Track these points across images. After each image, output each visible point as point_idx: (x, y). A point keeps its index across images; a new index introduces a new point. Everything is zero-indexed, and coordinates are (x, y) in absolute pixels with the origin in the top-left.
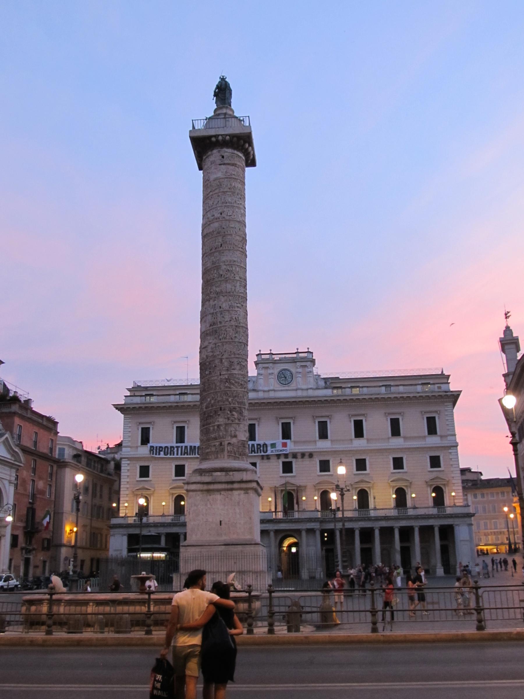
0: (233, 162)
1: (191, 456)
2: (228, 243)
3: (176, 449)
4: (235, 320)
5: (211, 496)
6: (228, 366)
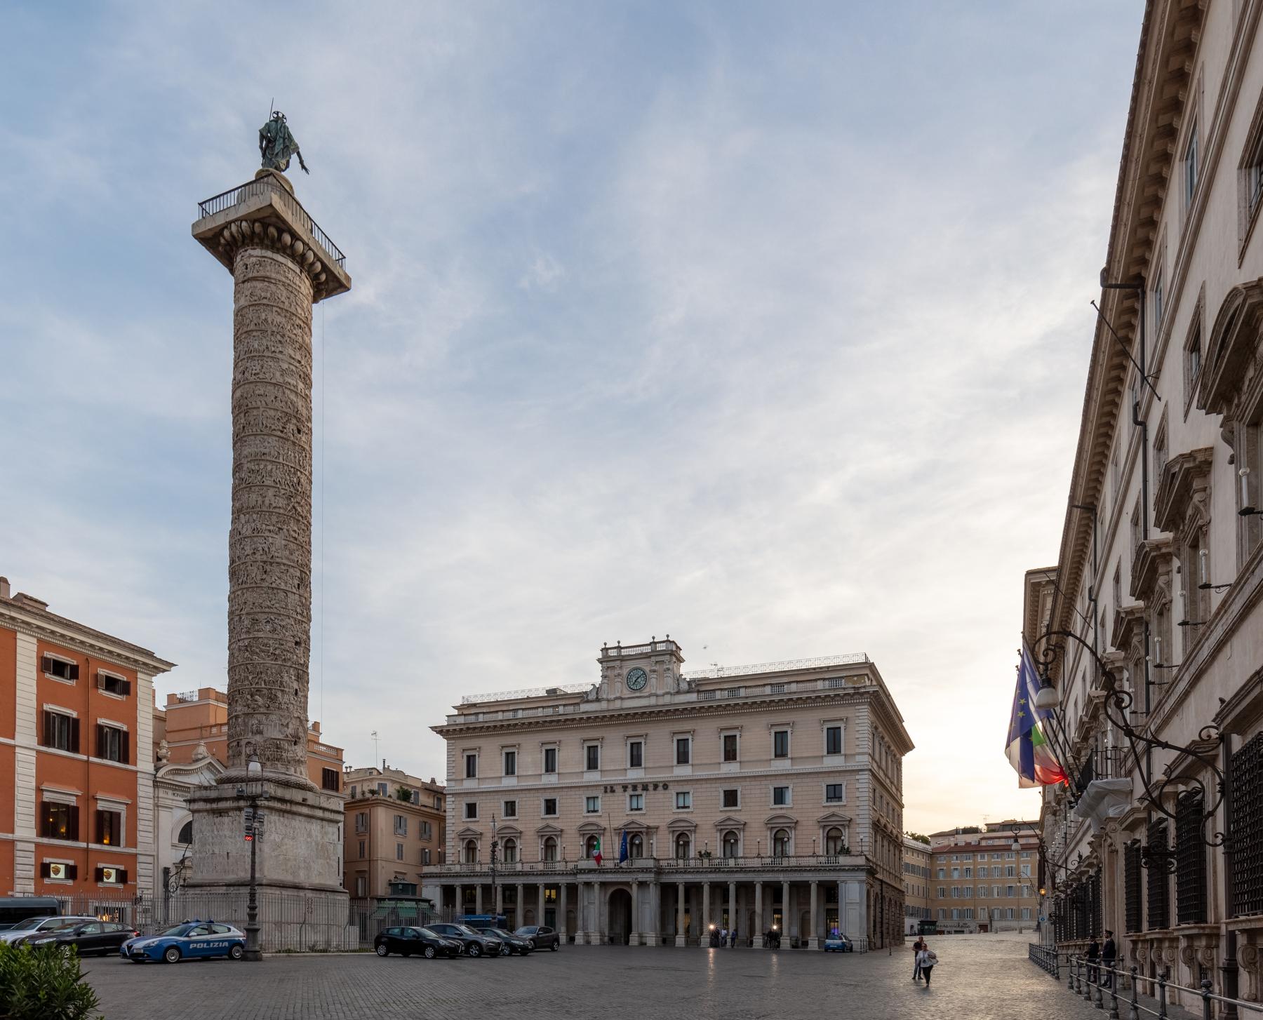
0: (262, 273)
4: (261, 552)
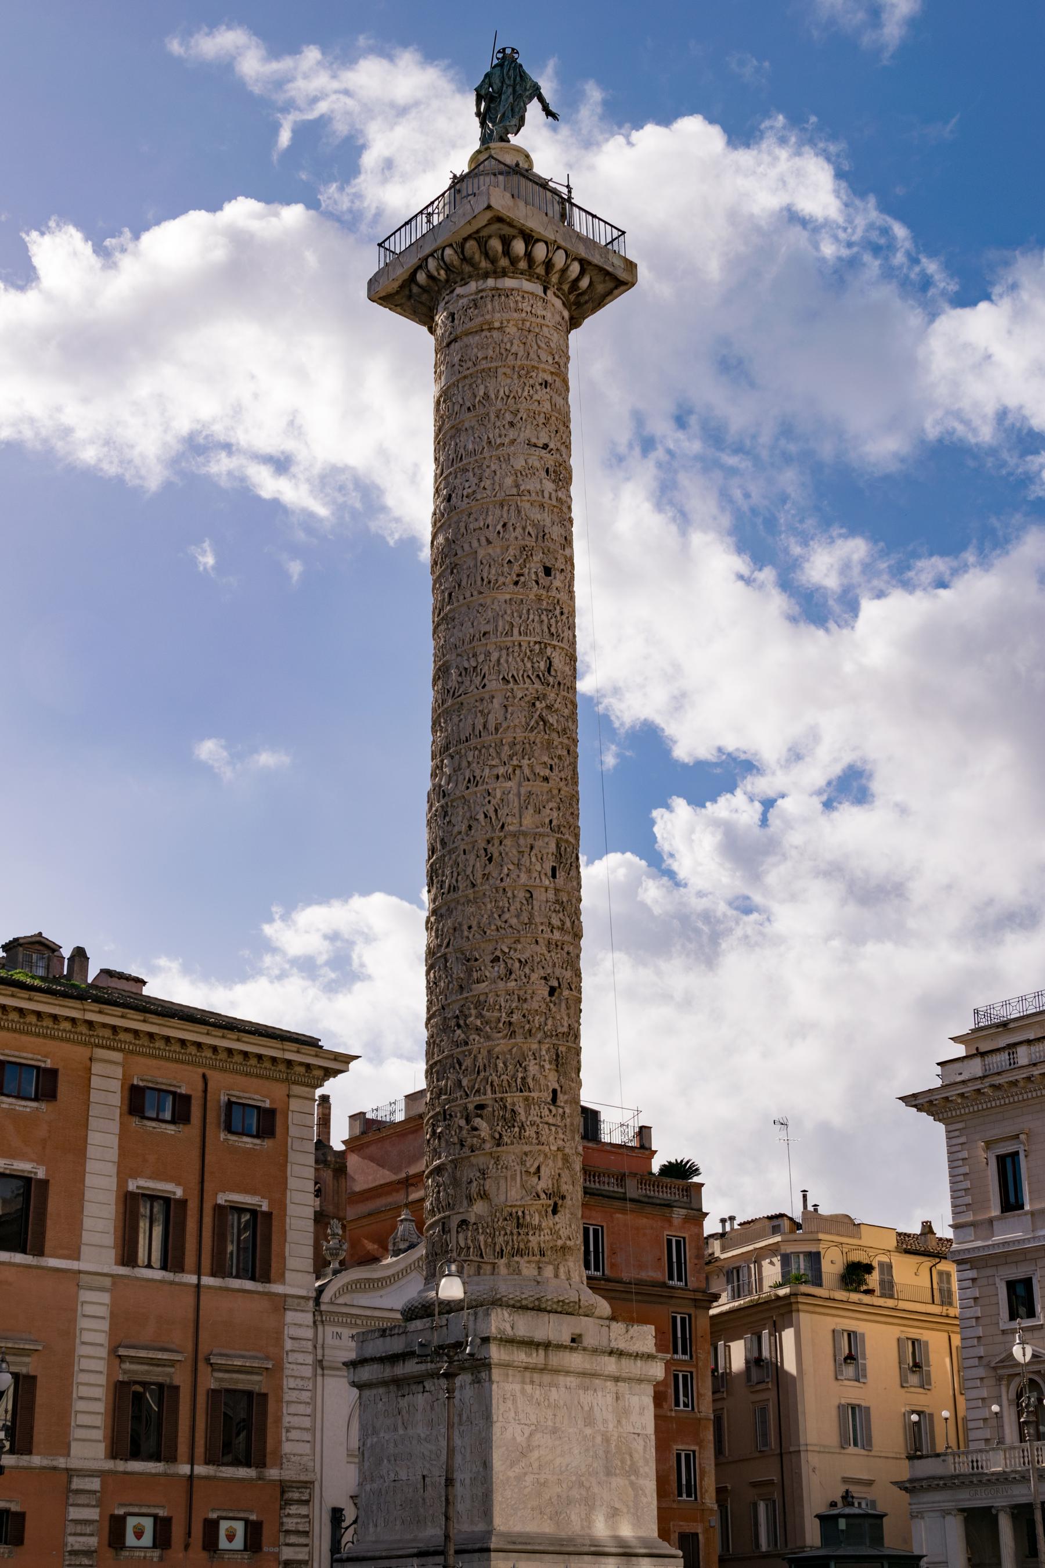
2: (464, 583)
6: (462, 976)
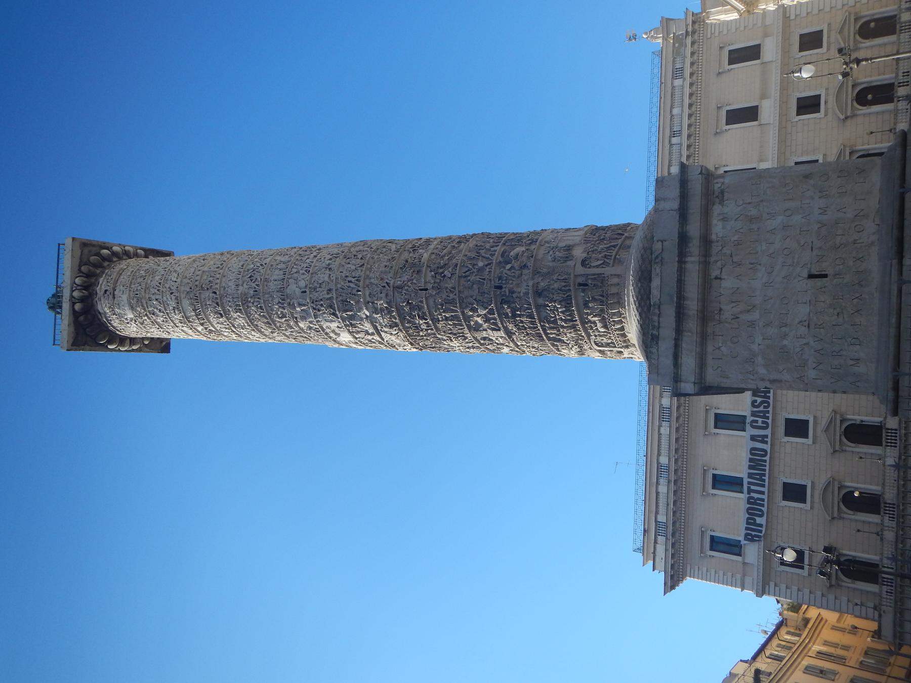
1: (767, 468)
3: (753, 495)
5: (723, 307)
